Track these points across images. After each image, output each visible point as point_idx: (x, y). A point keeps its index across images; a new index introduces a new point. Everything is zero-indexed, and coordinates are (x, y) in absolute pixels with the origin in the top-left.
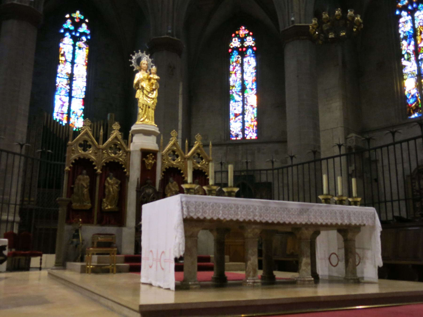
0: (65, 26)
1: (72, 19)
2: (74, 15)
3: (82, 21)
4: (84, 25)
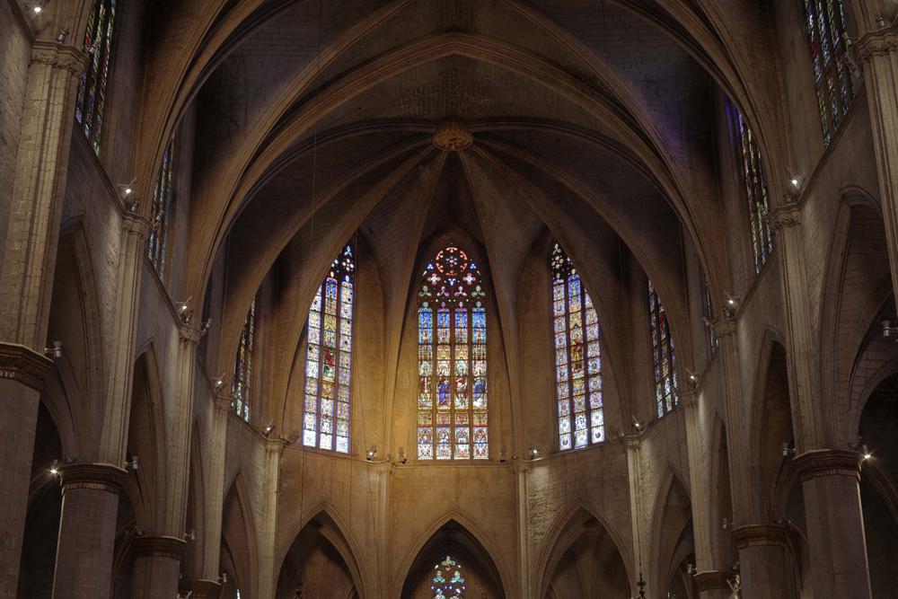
0: (436, 580)
1: (442, 568)
2: (444, 563)
3: (454, 569)
4: (457, 574)
